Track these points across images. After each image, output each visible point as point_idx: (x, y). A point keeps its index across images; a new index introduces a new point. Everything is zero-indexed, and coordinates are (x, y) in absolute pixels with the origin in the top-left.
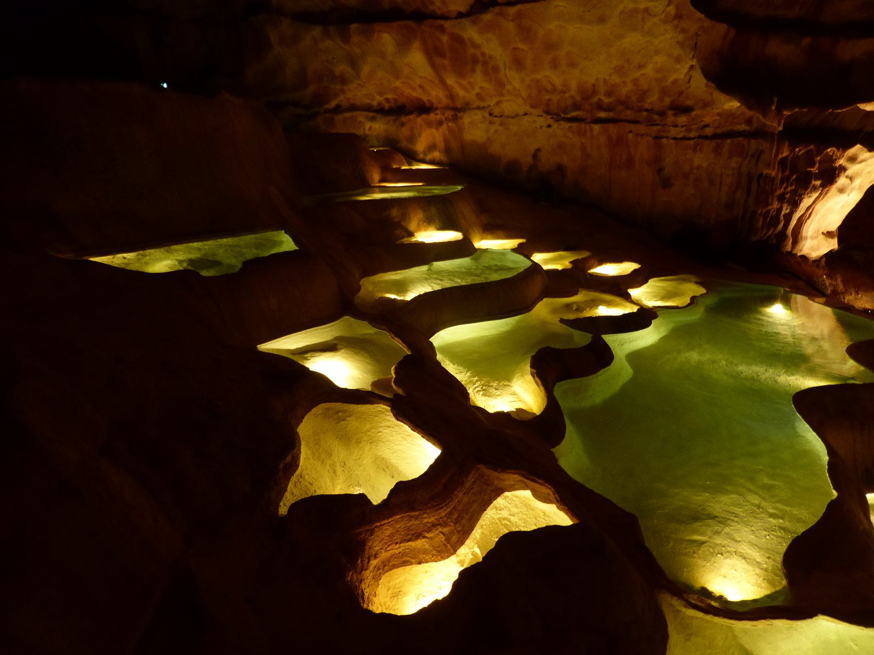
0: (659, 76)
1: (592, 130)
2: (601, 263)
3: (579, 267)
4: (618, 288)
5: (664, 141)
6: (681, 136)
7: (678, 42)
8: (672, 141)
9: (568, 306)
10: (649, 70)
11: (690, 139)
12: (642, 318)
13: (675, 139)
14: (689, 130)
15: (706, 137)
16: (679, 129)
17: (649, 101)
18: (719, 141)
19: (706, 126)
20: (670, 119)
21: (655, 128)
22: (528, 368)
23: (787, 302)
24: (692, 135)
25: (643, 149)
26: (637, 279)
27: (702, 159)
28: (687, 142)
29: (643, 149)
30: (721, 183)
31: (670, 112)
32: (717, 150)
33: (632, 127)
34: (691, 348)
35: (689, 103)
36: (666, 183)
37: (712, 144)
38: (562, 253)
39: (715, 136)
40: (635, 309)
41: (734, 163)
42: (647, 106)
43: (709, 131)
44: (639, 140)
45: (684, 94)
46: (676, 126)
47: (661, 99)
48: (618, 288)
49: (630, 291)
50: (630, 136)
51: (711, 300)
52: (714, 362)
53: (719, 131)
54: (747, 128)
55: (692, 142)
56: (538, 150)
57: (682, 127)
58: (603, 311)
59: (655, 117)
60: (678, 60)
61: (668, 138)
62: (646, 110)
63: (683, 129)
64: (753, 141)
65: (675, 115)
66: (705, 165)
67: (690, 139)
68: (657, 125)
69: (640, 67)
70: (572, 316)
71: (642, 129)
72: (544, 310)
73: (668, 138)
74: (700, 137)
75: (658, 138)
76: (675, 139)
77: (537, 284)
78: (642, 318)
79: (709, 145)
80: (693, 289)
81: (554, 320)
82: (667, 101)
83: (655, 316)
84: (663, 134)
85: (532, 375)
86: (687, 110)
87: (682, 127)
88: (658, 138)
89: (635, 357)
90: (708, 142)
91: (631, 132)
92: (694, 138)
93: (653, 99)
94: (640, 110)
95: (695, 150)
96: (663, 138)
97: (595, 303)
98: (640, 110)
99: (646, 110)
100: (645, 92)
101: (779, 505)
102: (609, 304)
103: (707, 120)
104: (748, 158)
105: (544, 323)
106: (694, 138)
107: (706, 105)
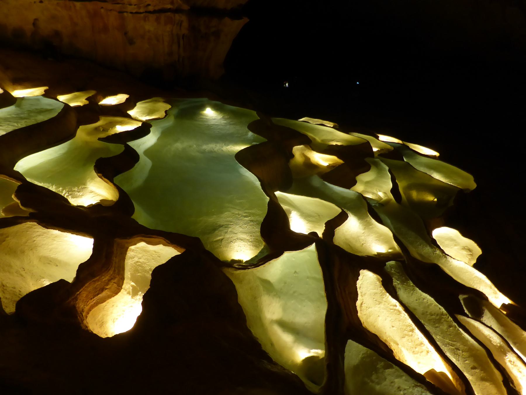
1: (75, 6)
2: (104, 97)
3: (93, 101)
4: (120, 112)
5: (125, 14)
6: (134, 11)
8: (130, 15)
9: (97, 129)
11: (141, 13)
12: (144, 129)
13: (131, 13)
14: (139, 8)
15: (150, 12)
16: (133, 6)
19: (149, 5)
21: (118, 5)
22: (94, 174)
23: (216, 108)
24: (142, 10)
25: (112, 20)
26: (130, 104)
27: (150, 26)
28: (139, 15)
29: (112, 20)
32: (157, 20)
34: (176, 141)
36: (131, 42)
38: (76, 93)
39: (154, 12)
40: (140, 124)
41: (168, 28)
43: (151, 8)
48: (120, 112)
49: (130, 112)
50: (102, 10)
51: (175, 111)
52: (190, 147)
53: (157, 8)
55: (142, 15)
56: (36, 20)
58: (120, 129)
61: (127, 12)
63: (136, 7)
64: (177, 15)
67: (141, 13)
68: (118, 3)
70: (103, 135)
72: (82, 133)
73: (127, 12)
74: (146, 12)
75: (121, 12)
76: (131, 13)
77: (73, 118)
78: (144, 129)
79: (152, 17)
80: (163, 107)
81: (93, 140)
83: (151, 126)
85: (100, 177)
87: (135, 5)
88: (121, 12)
89: (149, 152)
90: (152, 15)
91: (102, 8)
97: (113, 124)
101: (247, 211)
102: (121, 123)
105: (87, 143)
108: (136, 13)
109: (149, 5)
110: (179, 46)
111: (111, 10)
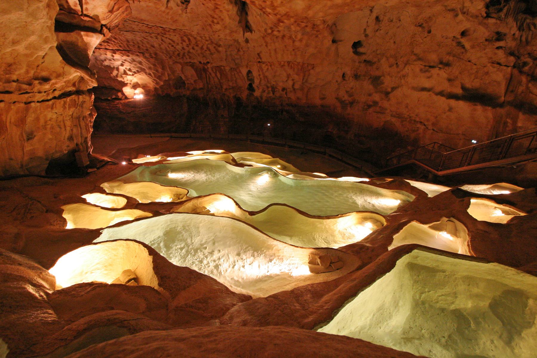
0: (28, 52)
5: (33, 104)
7: (47, 26)
8: (38, 104)
10: (21, 48)
11: (48, 100)
13: (38, 102)
14: (48, 94)
15: (55, 98)
17: (17, 73)
18: (65, 99)
20: (37, 85)
21: (27, 96)
24: (49, 98)
28: (47, 103)
30: (65, 126)
31: (37, 82)
33: (6, 97)
35: (44, 74)
36: (30, 137)
37: (62, 101)
39: (61, 97)
42: (15, 77)
43: (57, 94)
44: (12, 107)
45: (39, 68)
46: (40, 92)
47: (27, 72)
54: (74, 89)
55: (50, 103)
57: (45, 92)
59: (25, 86)
60: (46, 40)
62: (14, 81)
63: (45, 94)
64: (81, 97)
65: (40, 83)
66: (55, 116)
67: (48, 100)
68: (27, 93)
69: (14, 43)
71: (14, 97)
76: (38, 102)
82: (32, 73)
84: (30, 100)
86: (46, 80)
87: (45, 92)
92: (51, 100)
93: (20, 73)
94: (8, 81)
95: (52, 108)
96: (30, 102)
98: (8, 81)
99: (14, 81)
100: (10, 65)
103: (58, 86)
104: (78, 107)
106: (51, 100)
107: (59, 76)
108: (43, 101)
109: (55, 90)
110: (81, 128)
111: (14, 102)
